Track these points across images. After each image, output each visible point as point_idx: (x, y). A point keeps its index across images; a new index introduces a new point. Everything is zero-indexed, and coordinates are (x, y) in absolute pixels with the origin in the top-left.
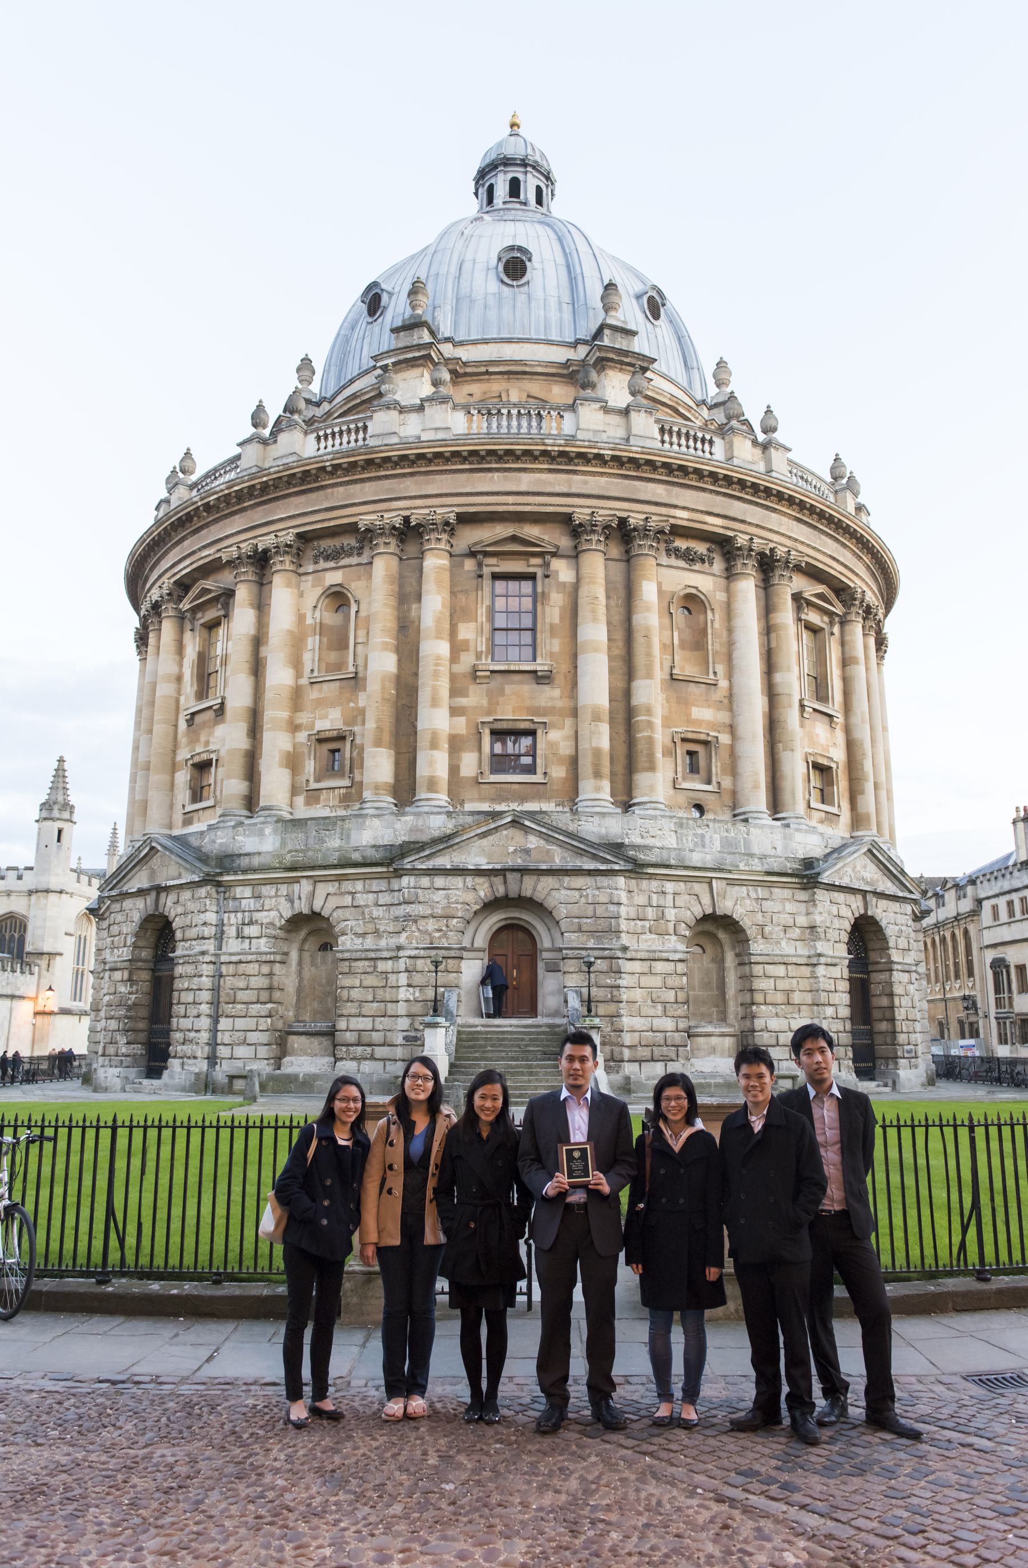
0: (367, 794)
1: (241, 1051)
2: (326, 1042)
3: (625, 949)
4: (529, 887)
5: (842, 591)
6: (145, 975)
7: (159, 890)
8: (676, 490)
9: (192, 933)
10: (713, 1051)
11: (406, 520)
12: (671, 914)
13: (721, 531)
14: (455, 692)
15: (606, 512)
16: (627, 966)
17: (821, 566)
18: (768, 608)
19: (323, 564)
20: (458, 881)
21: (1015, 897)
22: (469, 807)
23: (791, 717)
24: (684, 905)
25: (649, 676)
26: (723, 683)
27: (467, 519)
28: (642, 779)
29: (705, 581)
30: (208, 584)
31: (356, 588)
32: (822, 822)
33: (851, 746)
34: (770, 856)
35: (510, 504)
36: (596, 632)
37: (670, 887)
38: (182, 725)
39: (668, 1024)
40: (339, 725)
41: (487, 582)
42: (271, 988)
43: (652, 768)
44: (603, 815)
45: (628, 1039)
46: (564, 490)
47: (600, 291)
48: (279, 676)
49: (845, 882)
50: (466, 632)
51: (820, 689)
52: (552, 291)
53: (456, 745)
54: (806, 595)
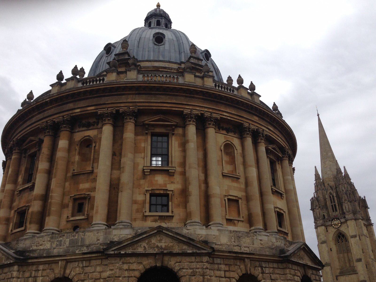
5: (180, 114)
13: (95, 111)
17: (154, 108)
26: (95, 171)
32: (155, 221)
34: (93, 245)
37: (41, 267)
49: (140, 250)
54: (146, 122)
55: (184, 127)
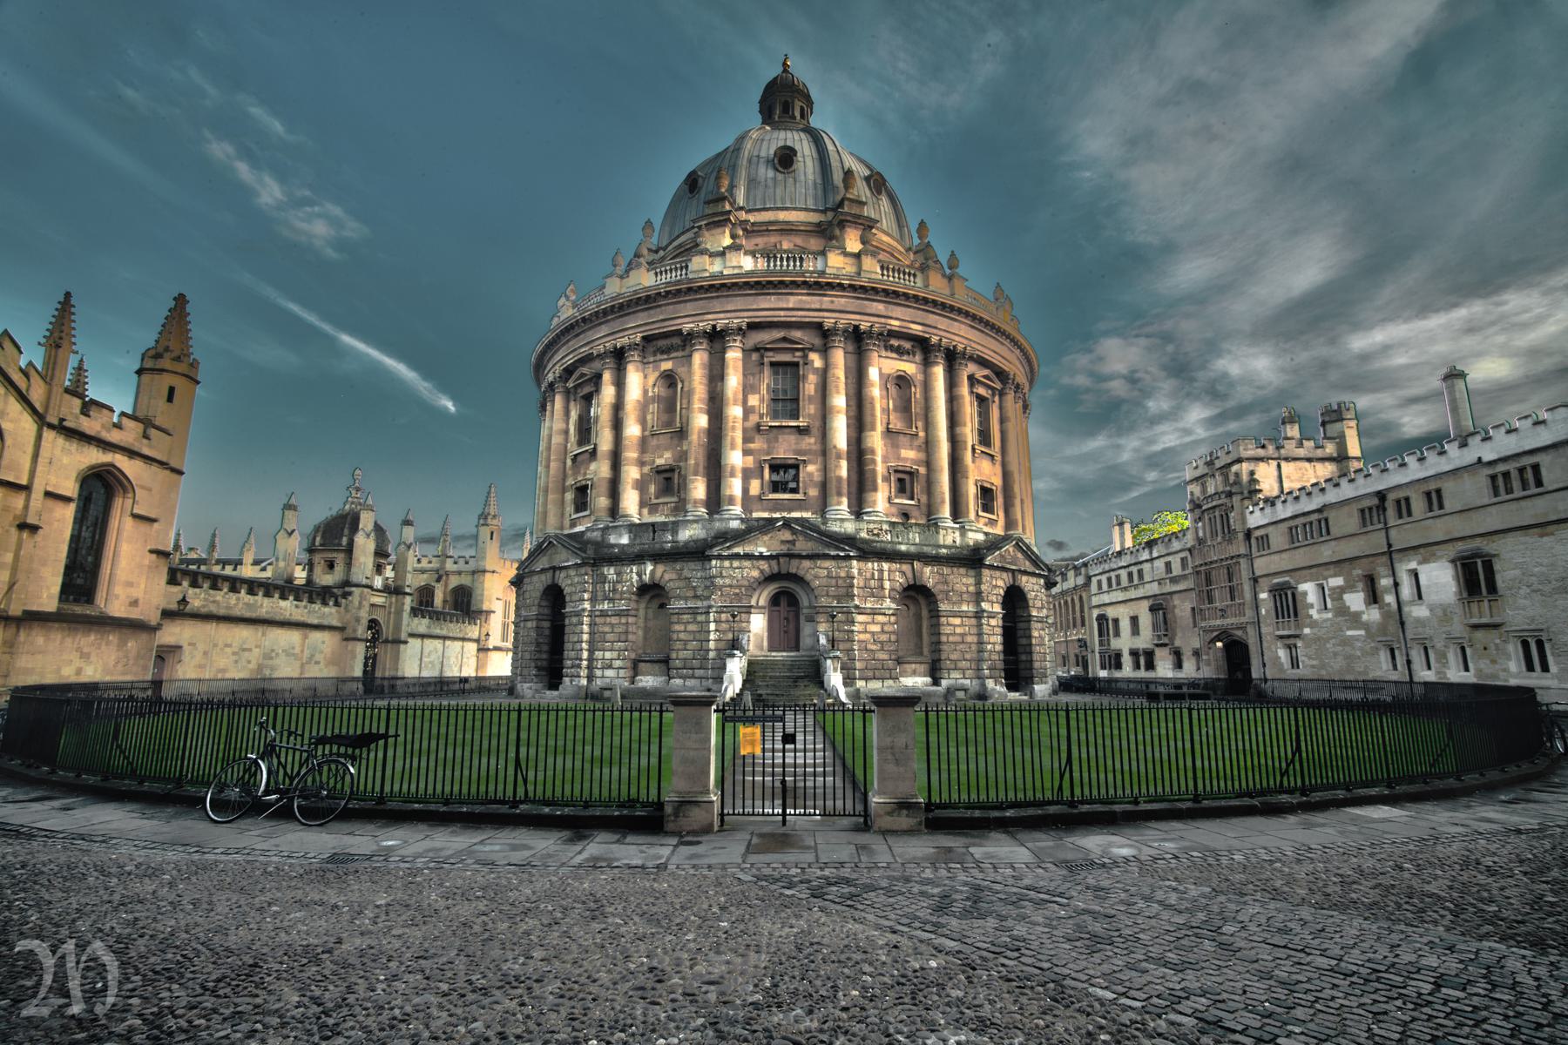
0: (689, 507)
1: (610, 673)
2: (663, 667)
3: (857, 607)
4: (794, 567)
5: (1001, 374)
6: (546, 624)
7: (554, 569)
8: (891, 307)
9: (575, 597)
10: (914, 673)
11: (714, 327)
12: (887, 585)
14: (746, 440)
15: (844, 321)
16: (860, 618)
18: (951, 385)
19: (659, 357)
20: (747, 563)
21: (1113, 575)
22: (755, 515)
23: (968, 456)
24: (893, 576)
25: (873, 429)
27: (753, 326)
28: (870, 496)
29: (910, 368)
30: (585, 370)
31: (681, 371)
33: (1006, 475)
35: (782, 316)
36: (839, 401)
38: (569, 462)
39: (882, 656)
40: (671, 462)
41: (767, 371)
42: (627, 632)
43: (875, 489)
44: (842, 520)
45: (858, 665)
46: (817, 306)
47: (841, 175)
48: (632, 430)
50: (753, 400)
51: (984, 437)
52: (811, 177)
53: (747, 475)
55: (1002, 394)
